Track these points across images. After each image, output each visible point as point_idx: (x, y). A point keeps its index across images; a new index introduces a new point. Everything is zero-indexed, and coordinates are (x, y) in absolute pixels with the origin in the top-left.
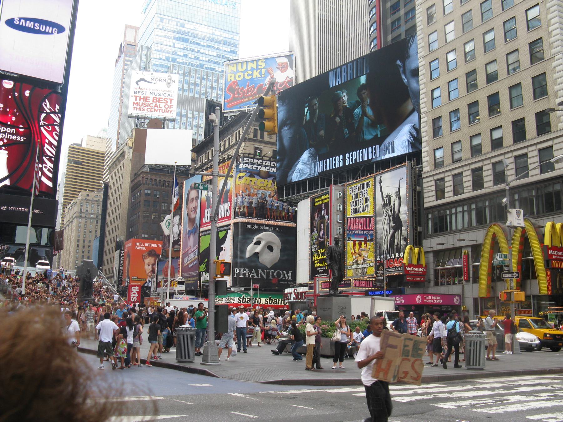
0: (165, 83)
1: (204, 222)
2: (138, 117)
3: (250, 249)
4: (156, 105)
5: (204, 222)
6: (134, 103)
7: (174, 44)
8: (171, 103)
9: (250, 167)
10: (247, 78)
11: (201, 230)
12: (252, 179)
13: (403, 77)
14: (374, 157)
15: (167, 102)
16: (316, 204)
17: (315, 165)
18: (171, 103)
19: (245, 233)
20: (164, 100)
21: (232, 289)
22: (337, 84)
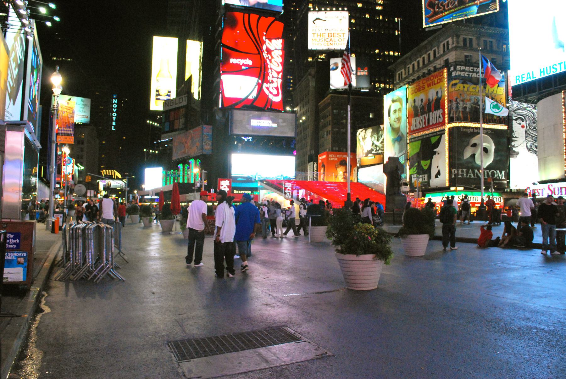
4: (331, 40)
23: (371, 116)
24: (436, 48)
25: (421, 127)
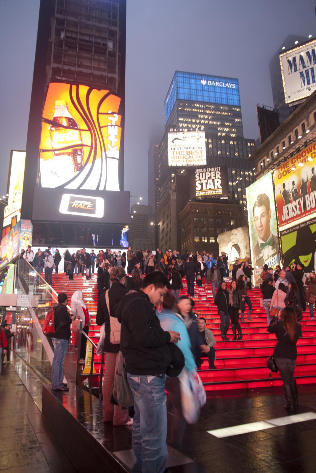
0: (195, 139)
1: (284, 219)
4: (190, 157)
5: (284, 219)
6: (172, 157)
8: (201, 153)
15: (198, 153)
18: (201, 153)
20: (196, 152)
23: (232, 224)
24: (305, 121)
25: (295, 215)
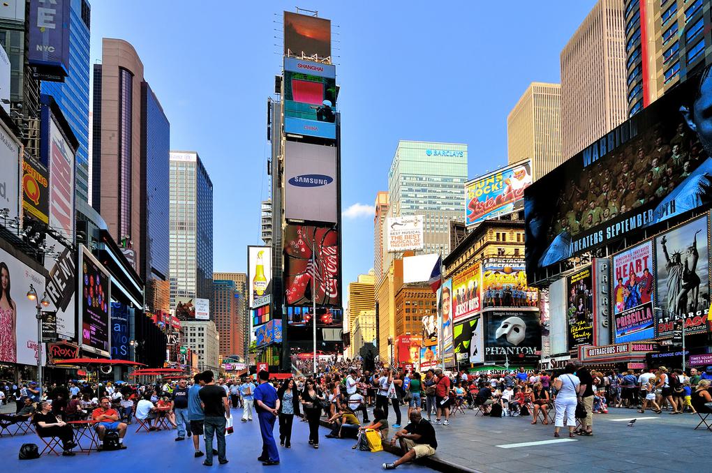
2: (395, 252)
3: (499, 332)
7: (416, 195)
9: (495, 265)
10: (485, 192)
11: (454, 322)
12: (497, 275)
13: (690, 123)
14: (645, 223)
16: (572, 282)
17: (569, 246)
19: (492, 320)
21: (485, 364)
22: (594, 161)
